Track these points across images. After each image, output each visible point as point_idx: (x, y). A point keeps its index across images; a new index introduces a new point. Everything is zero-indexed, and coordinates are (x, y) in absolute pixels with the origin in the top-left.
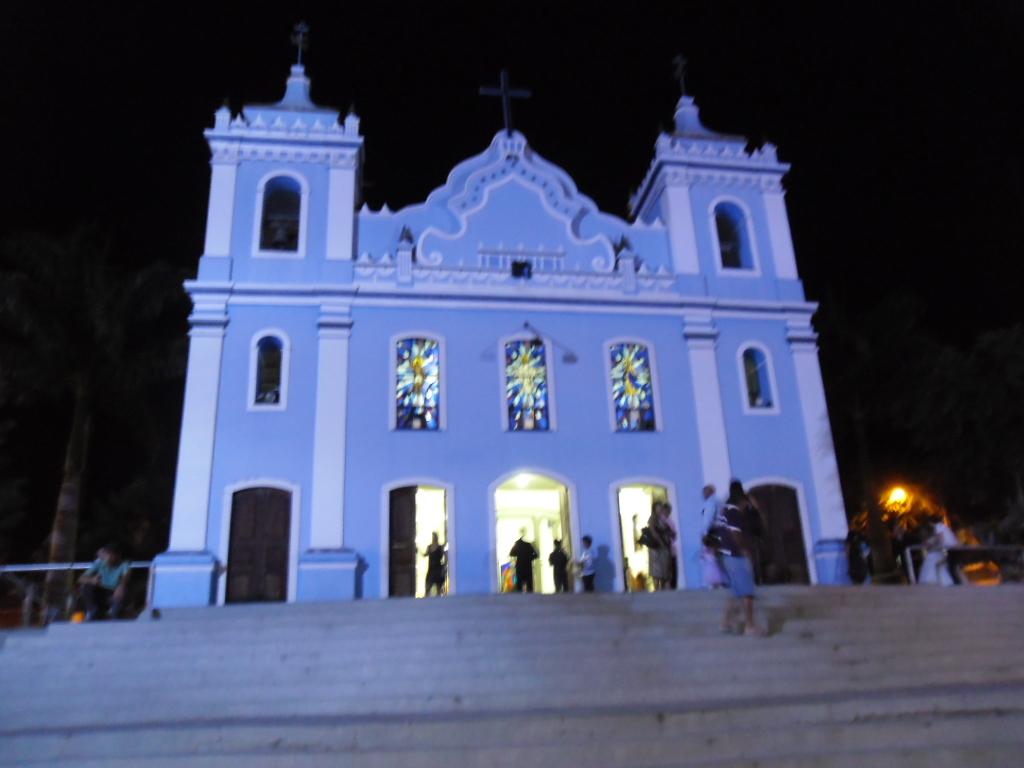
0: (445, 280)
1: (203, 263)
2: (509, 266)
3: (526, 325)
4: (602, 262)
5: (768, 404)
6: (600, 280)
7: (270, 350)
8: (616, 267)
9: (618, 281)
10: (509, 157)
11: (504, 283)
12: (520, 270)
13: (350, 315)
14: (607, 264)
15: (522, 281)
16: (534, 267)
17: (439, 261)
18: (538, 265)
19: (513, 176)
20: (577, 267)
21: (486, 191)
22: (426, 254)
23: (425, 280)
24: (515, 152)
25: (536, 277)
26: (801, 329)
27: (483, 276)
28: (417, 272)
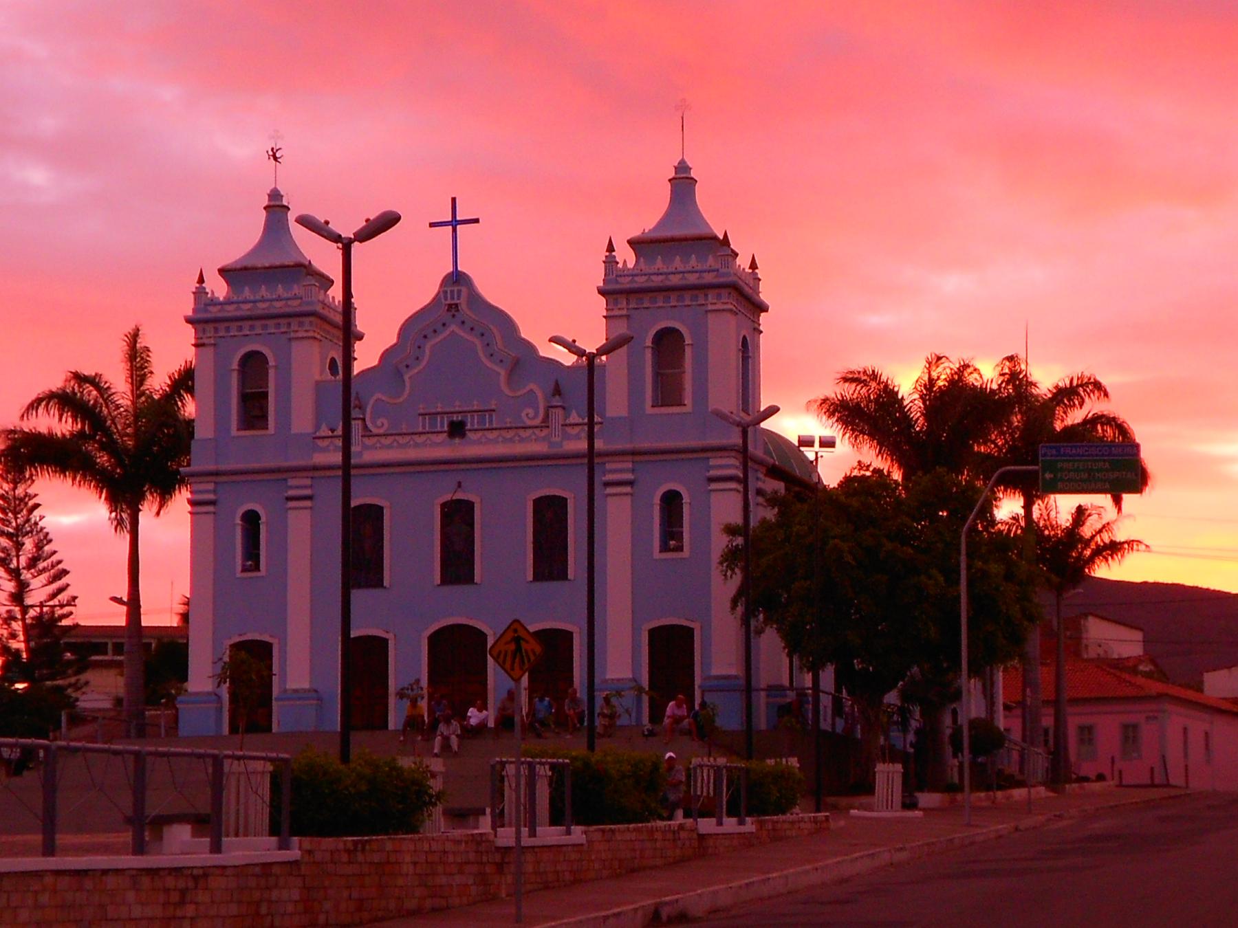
0: (390, 447)
1: (194, 446)
2: (446, 428)
3: (459, 485)
4: (532, 414)
5: (680, 549)
6: (529, 431)
7: (251, 519)
8: (546, 418)
9: (545, 432)
10: (450, 306)
11: (438, 444)
12: (457, 430)
13: (311, 487)
14: (534, 418)
15: (457, 440)
16: (469, 427)
17: (386, 425)
18: (472, 424)
19: (454, 327)
20: (508, 422)
21: (428, 346)
22: (374, 423)
23: (374, 447)
24: (456, 301)
25: (470, 435)
26: (728, 467)
27: (423, 438)
28: (366, 440)
